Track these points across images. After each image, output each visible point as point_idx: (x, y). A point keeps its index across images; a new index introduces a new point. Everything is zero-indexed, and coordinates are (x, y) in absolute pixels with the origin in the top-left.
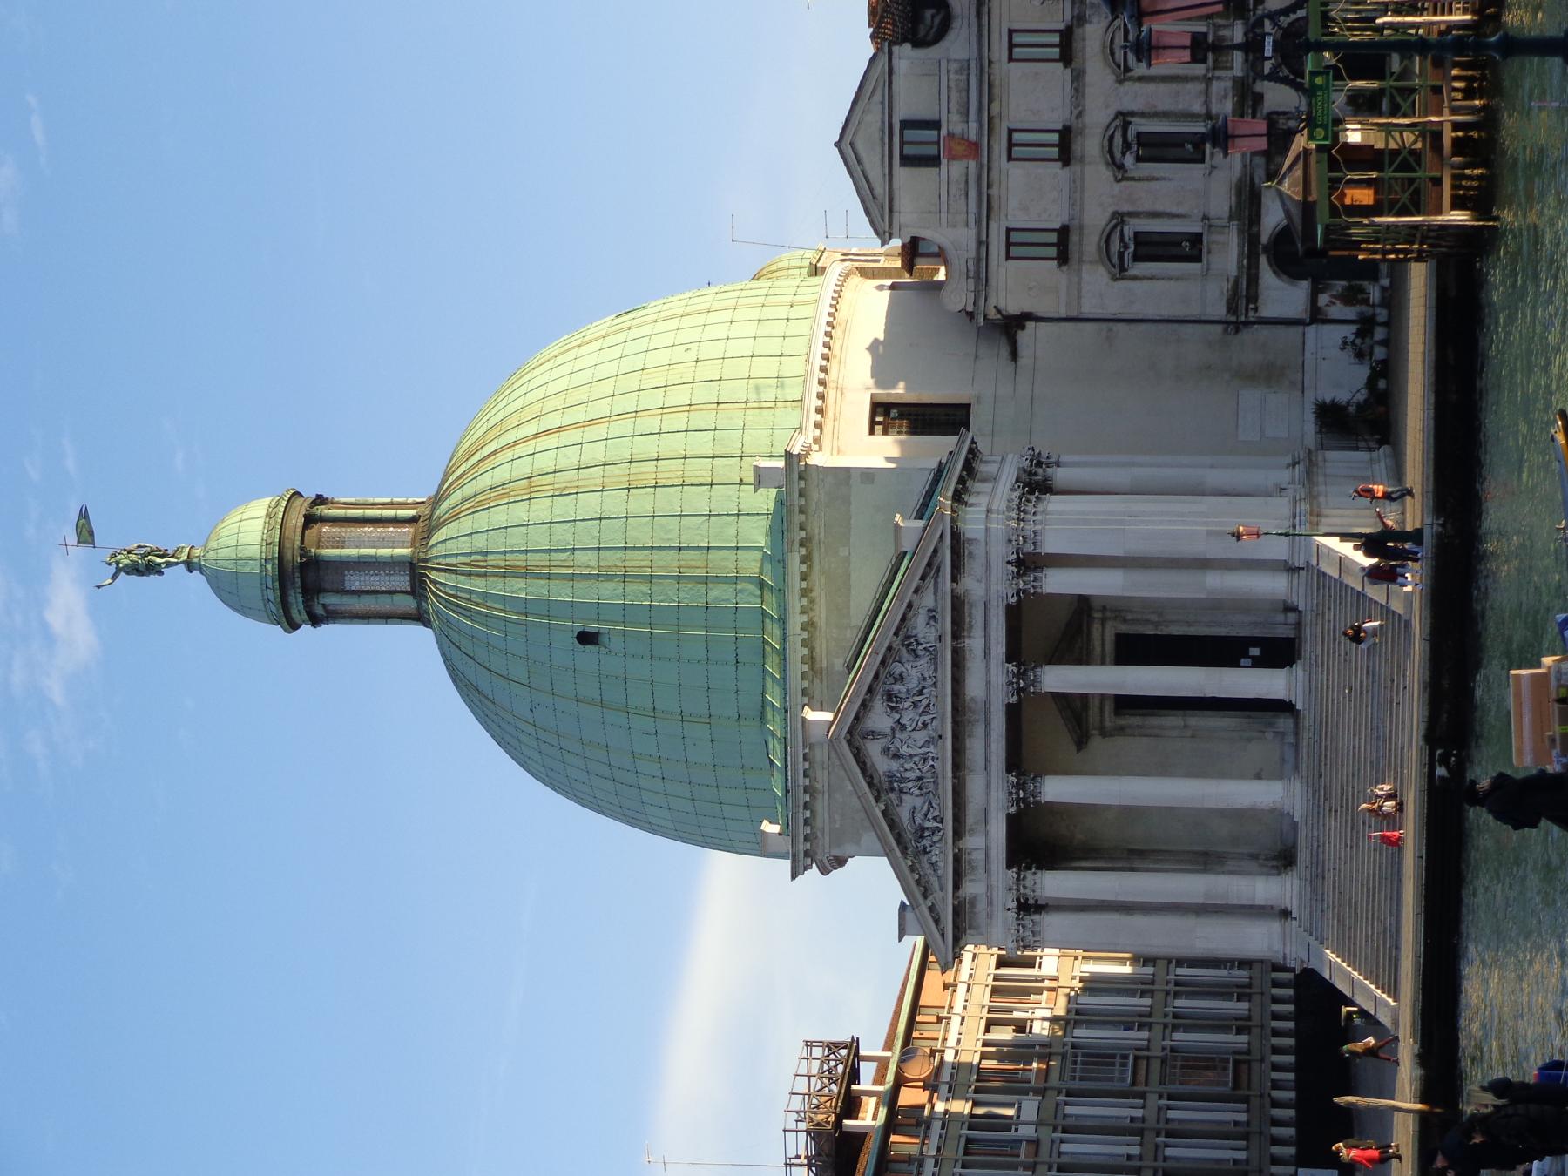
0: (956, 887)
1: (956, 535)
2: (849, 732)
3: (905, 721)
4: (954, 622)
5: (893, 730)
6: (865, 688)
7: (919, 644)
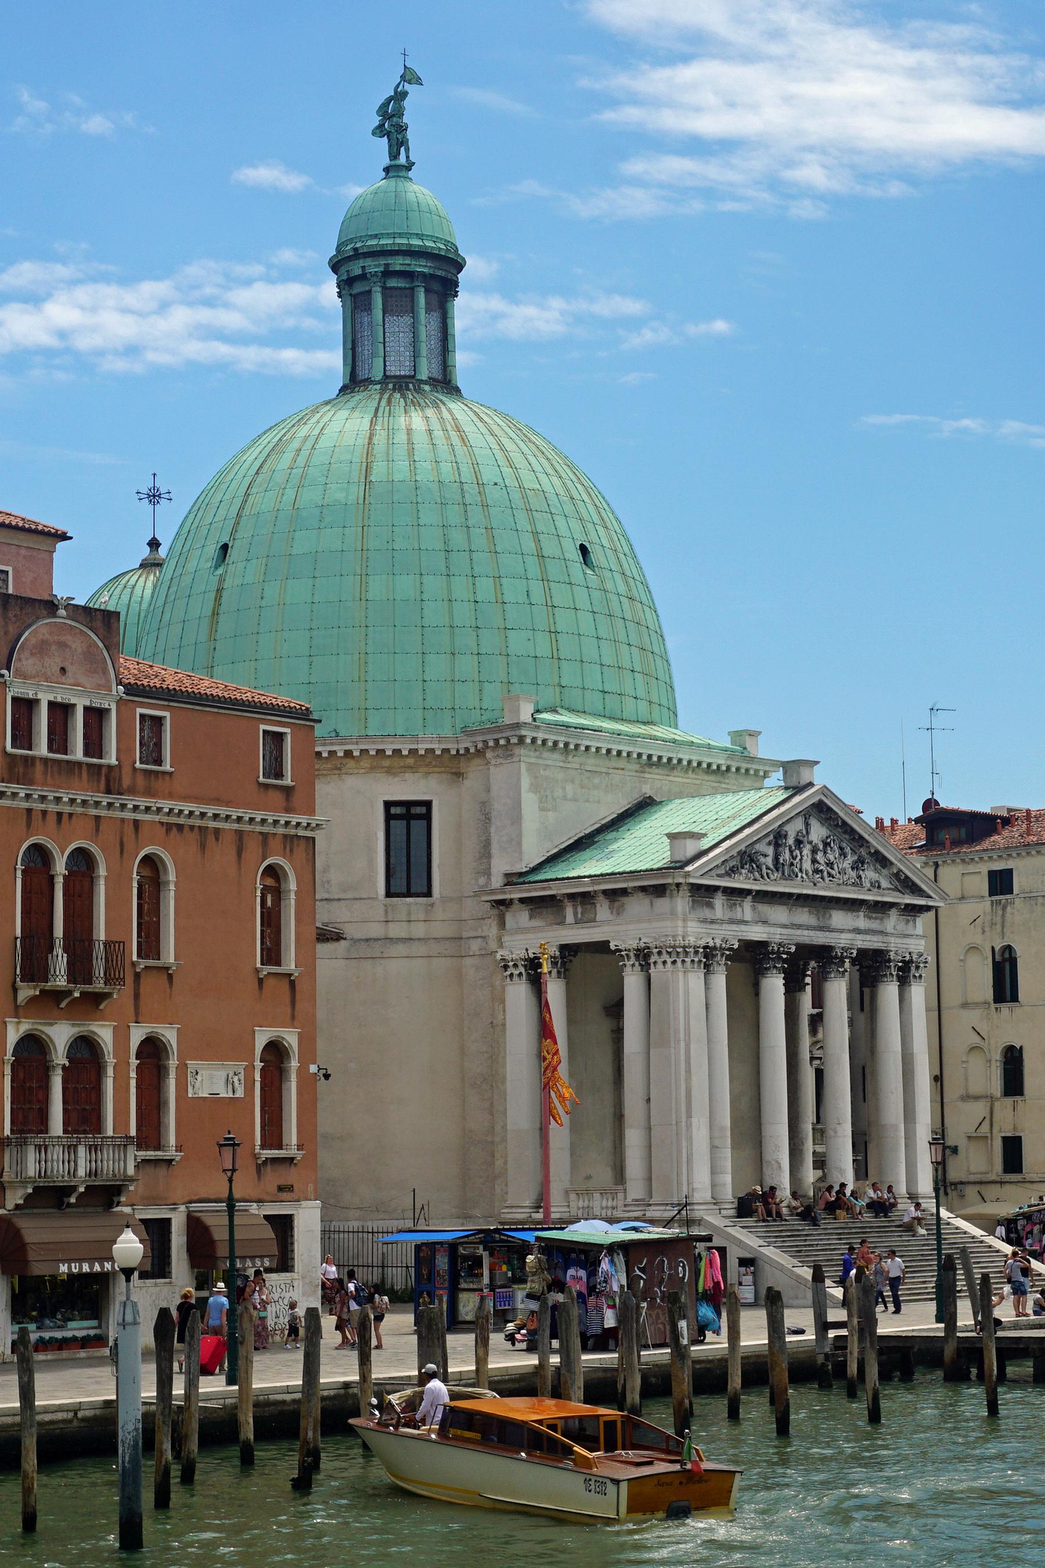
5: (810, 843)
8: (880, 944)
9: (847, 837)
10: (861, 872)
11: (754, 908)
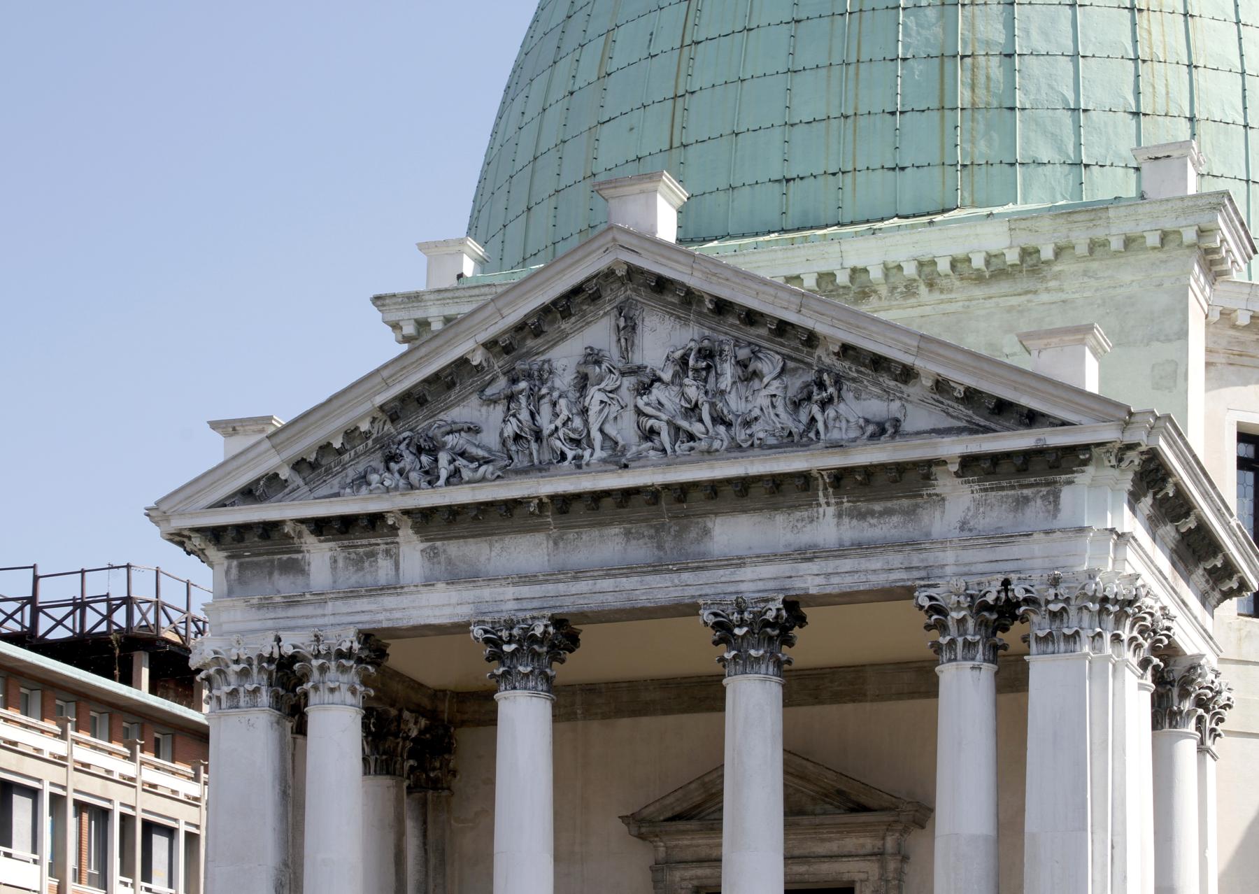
0: (320, 526)
1: (1068, 459)
2: (633, 272)
3: (657, 392)
4: (869, 472)
6: (725, 294)
7: (824, 405)
8: (904, 575)
9: (763, 331)
10: (816, 409)
11: (432, 555)
